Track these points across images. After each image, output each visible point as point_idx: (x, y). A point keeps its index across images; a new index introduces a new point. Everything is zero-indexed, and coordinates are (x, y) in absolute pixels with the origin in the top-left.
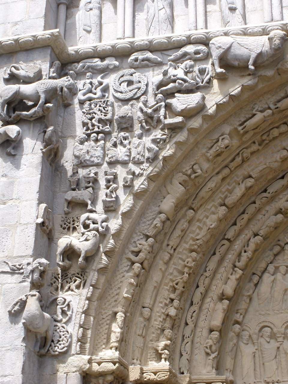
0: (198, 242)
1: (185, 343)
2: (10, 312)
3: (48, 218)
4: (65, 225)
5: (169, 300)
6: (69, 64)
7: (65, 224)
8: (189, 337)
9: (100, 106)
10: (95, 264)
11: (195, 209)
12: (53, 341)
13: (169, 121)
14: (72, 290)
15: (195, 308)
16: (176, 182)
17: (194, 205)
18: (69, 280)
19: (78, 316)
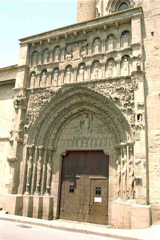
16: (44, 115)
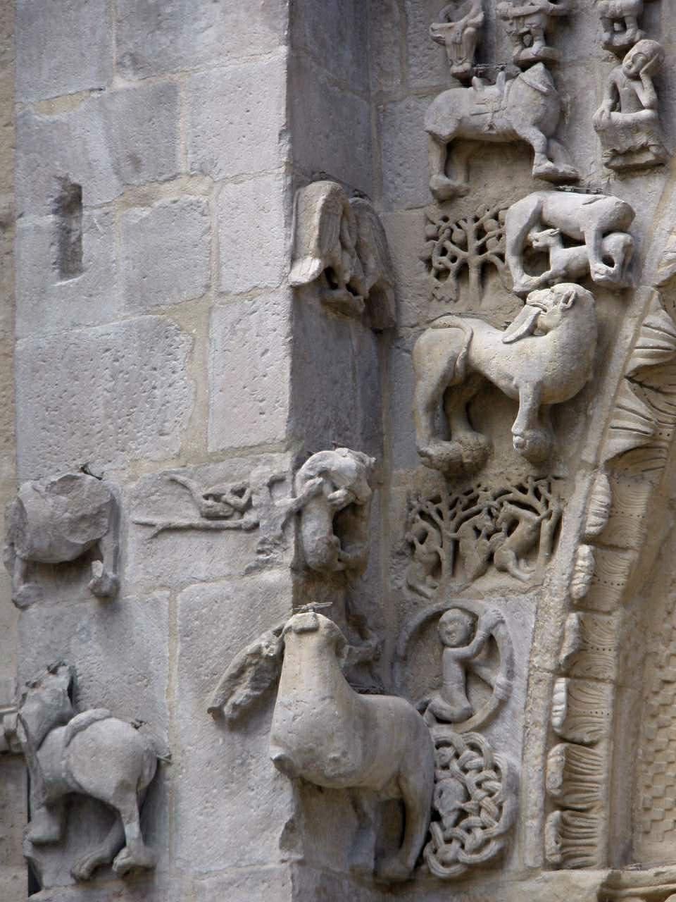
2: (216, 713)
3: (350, 243)
4: (445, 259)
7: (444, 252)
10: (593, 439)
12: (436, 817)
14: (503, 570)
18: (484, 521)
19: (539, 691)
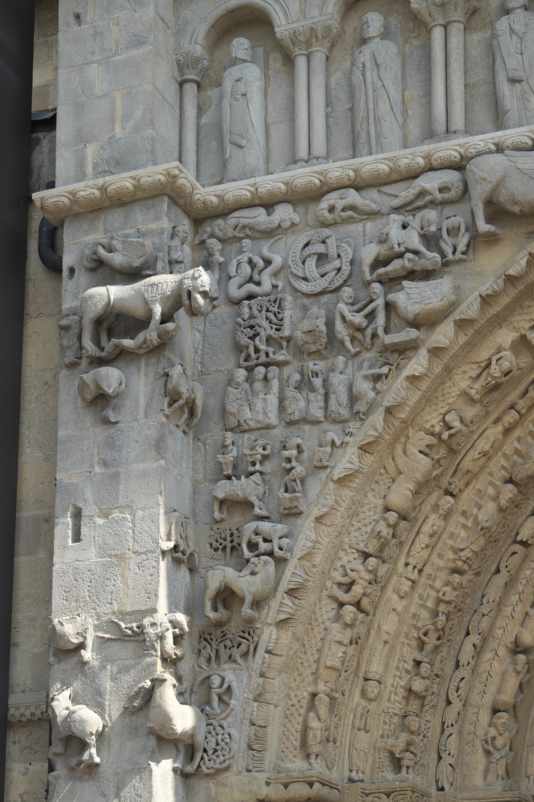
0: (462, 554)
1: (446, 736)
3: (184, 536)
5: (411, 663)
6: (209, 220)
8: (452, 725)
9: (268, 310)
10: (271, 614)
11: (454, 493)
13: (390, 339)
14: (235, 662)
15: (463, 672)
17: (453, 486)
